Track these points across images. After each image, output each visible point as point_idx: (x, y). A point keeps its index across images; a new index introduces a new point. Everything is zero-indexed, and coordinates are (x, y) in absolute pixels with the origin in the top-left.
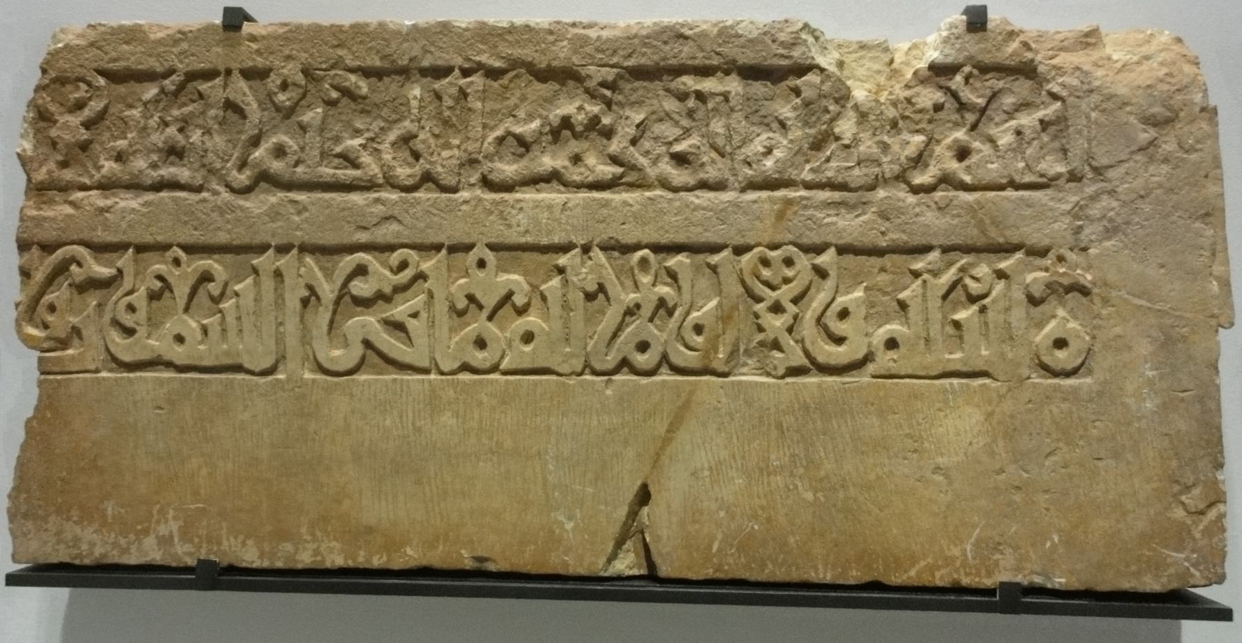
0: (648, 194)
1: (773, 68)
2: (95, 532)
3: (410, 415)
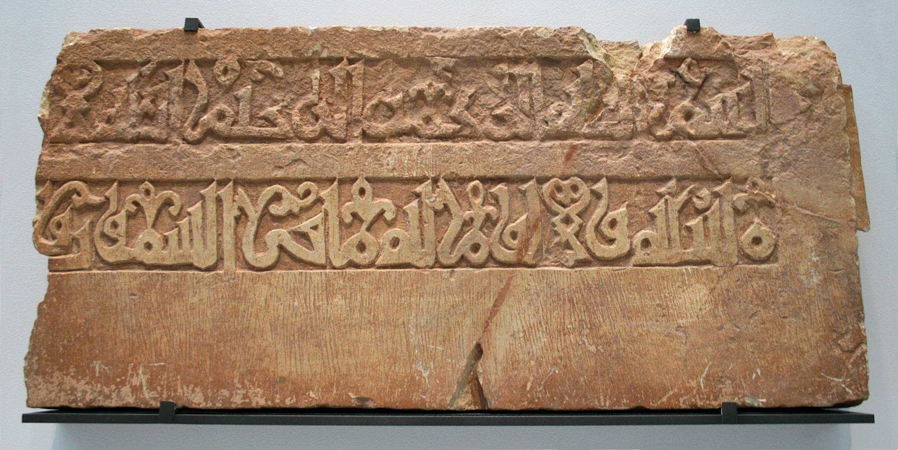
0: (477, 143)
1: (561, 57)
2: (87, 383)
3: (312, 298)
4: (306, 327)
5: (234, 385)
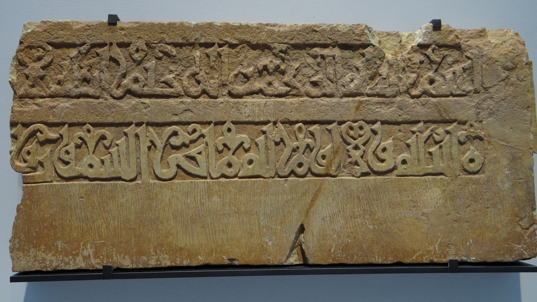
0: (301, 99)
1: (353, 44)
2: (53, 255)
3: (199, 197)
4: (196, 216)
5: (150, 253)
